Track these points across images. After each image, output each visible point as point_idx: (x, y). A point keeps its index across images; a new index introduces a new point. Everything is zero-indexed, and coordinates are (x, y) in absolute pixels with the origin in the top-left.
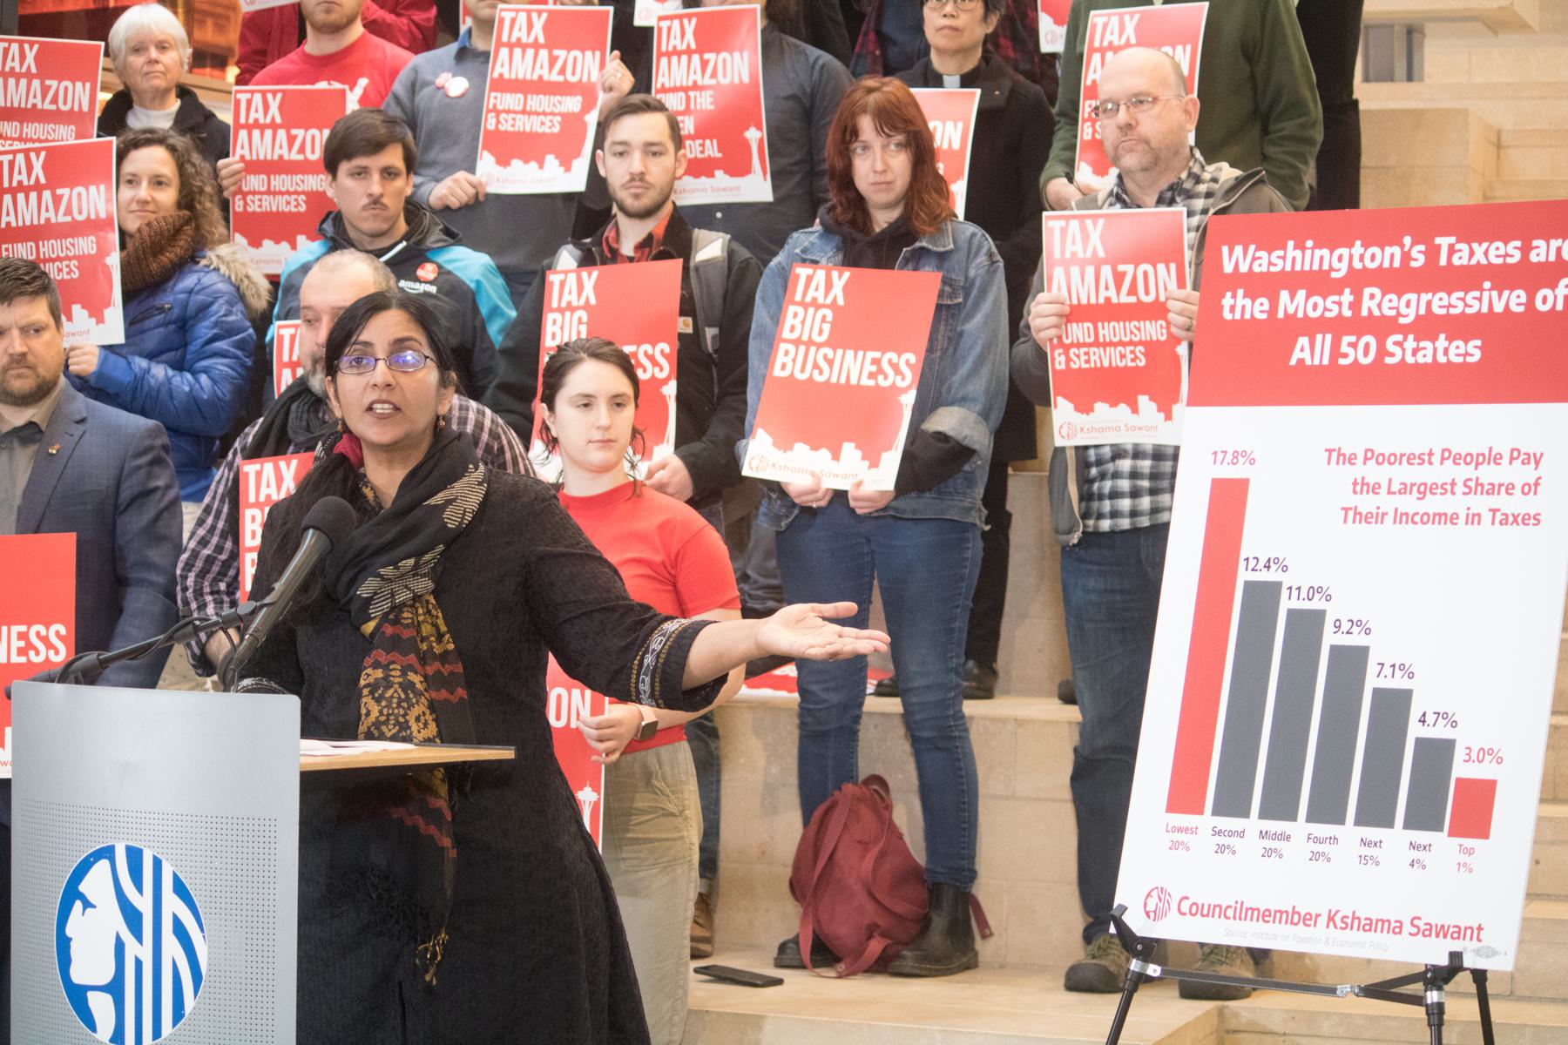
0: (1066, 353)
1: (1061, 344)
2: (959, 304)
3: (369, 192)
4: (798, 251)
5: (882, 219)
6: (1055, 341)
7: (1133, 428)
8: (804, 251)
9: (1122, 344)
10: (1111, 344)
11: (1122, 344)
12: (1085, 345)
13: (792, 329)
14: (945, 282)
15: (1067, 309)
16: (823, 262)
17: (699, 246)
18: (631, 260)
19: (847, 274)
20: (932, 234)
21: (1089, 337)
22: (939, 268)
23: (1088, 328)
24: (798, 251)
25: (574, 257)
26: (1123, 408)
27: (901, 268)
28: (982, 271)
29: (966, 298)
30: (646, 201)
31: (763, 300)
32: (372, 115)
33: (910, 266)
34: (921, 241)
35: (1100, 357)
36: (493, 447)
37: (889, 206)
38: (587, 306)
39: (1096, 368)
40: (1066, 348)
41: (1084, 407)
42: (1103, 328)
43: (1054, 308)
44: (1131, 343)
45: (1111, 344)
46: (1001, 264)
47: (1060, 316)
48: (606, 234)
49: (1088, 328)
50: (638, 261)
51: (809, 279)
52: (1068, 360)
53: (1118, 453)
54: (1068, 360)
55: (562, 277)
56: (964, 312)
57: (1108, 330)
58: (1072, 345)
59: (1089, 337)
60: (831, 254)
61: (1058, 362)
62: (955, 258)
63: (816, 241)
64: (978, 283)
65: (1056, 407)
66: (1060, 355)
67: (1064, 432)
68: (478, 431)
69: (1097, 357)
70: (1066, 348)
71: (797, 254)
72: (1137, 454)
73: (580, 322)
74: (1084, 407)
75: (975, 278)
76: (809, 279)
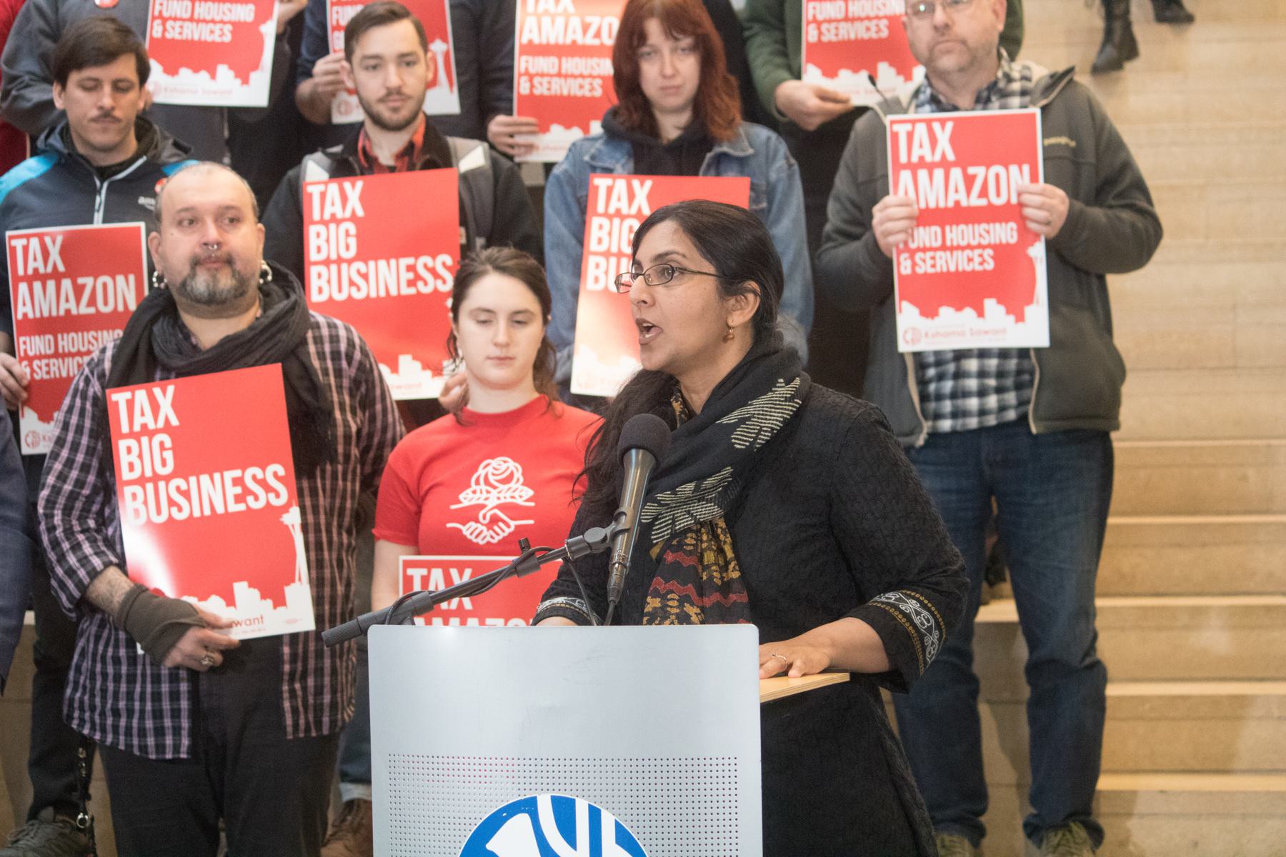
0: (912, 258)
1: (907, 248)
2: (762, 210)
3: (100, 104)
4: (587, 158)
5: (672, 126)
6: (901, 246)
7: (979, 333)
8: (593, 158)
9: (969, 247)
10: (959, 248)
11: (969, 247)
12: (932, 249)
13: (600, 241)
14: (753, 187)
15: (916, 212)
16: (619, 168)
17: (459, 154)
18: (392, 169)
19: (649, 183)
20: (729, 141)
21: (936, 240)
22: (742, 173)
23: (936, 233)
24: (587, 158)
25: (323, 167)
26: (969, 312)
27: (705, 174)
28: (784, 175)
29: (770, 202)
30: (405, 113)
31: (553, 208)
32: (105, 23)
33: (713, 171)
34: (720, 145)
35: (947, 262)
36: (365, 366)
37: (678, 110)
38: (353, 218)
39: (942, 273)
40: (912, 253)
41: (929, 311)
42: (951, 231)
43: (903, 211)
44: (980, 246)
45: (959, 248)
46: (796, 167)
47: (909, 218)
48: (360, 145)
49: (936, 233)
50: (400, 171)
51: (610, 190)
52: (914, 264)
53: (960, 355)
54: (914, 264)
55: (322, 188)
56: (772, 216)
57: (956, 234)
58: (919, 249)
59: (936, 240)
60: (623, 161)
61: (903, 267)
62: (753, 163)
63: (603, 148)
64: (780, 188)
65: (900, 311)
66: (905, 259)
67: (909, 337)
68: (351, 349)
69: (943, 262)
70: (912, 253)
71: (587, 162)
72: (983, 354)
73: (347, 234)
74: (929, 311)
75: (778, 180)
76: (610, 190)
